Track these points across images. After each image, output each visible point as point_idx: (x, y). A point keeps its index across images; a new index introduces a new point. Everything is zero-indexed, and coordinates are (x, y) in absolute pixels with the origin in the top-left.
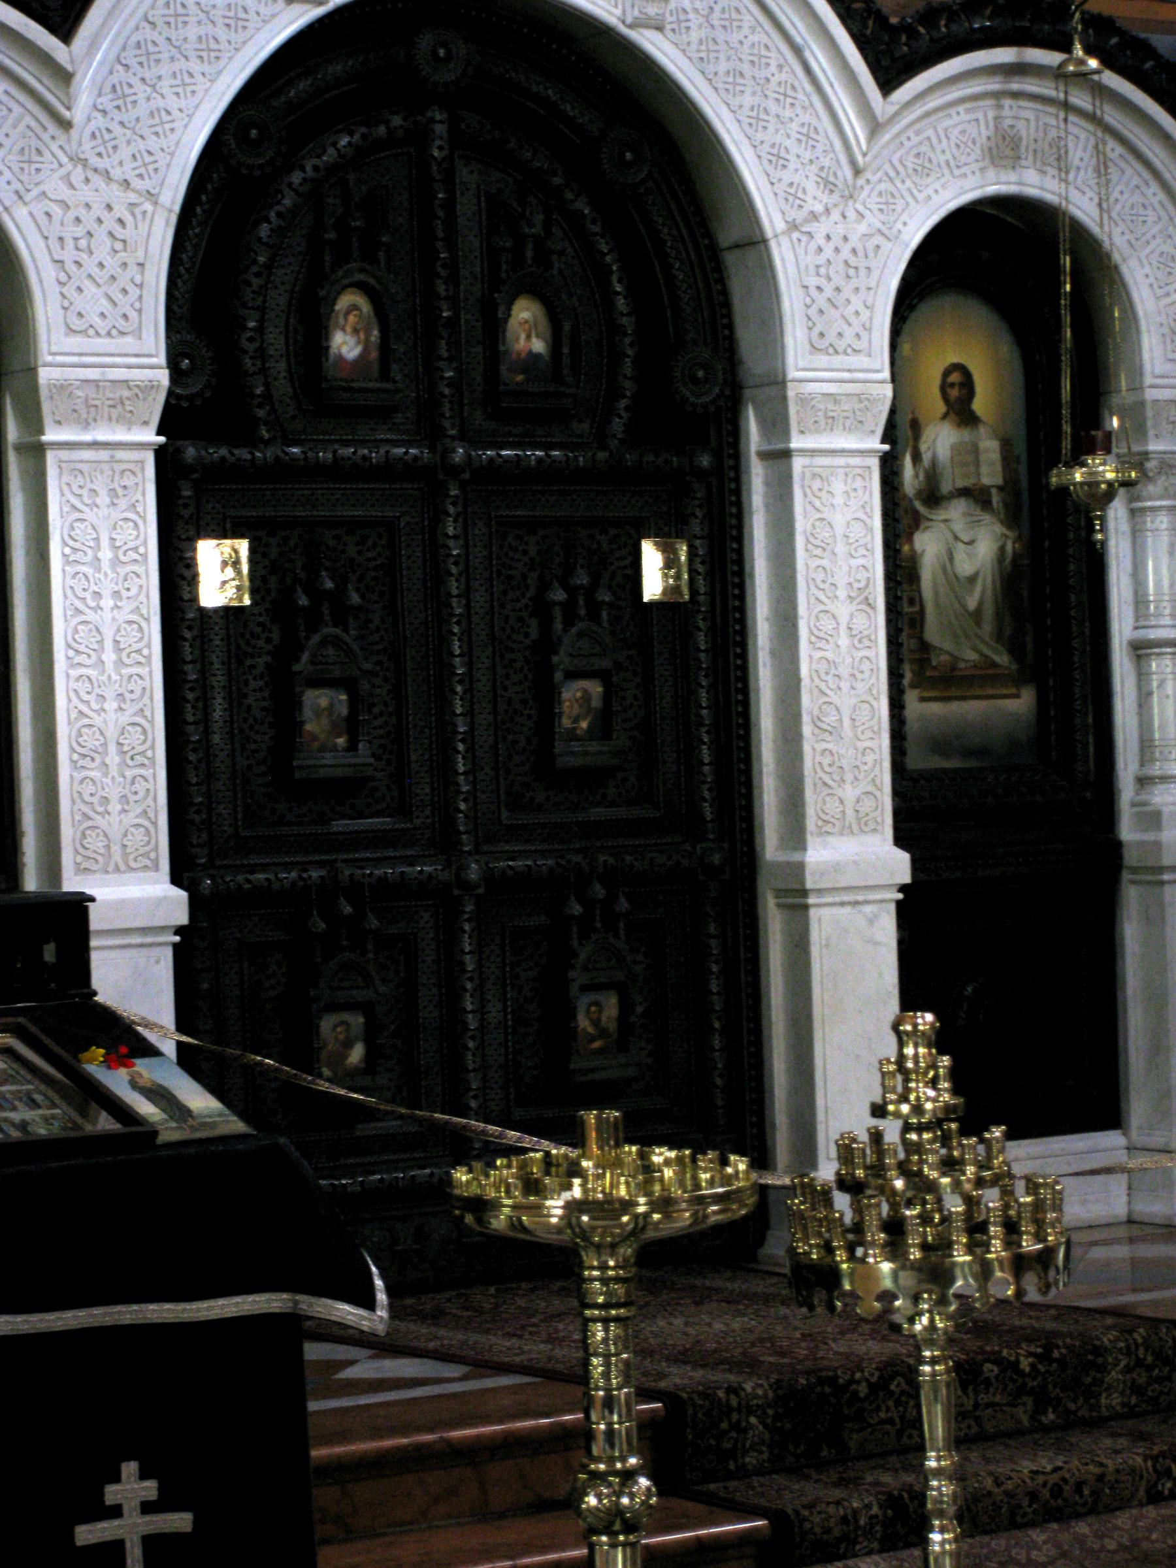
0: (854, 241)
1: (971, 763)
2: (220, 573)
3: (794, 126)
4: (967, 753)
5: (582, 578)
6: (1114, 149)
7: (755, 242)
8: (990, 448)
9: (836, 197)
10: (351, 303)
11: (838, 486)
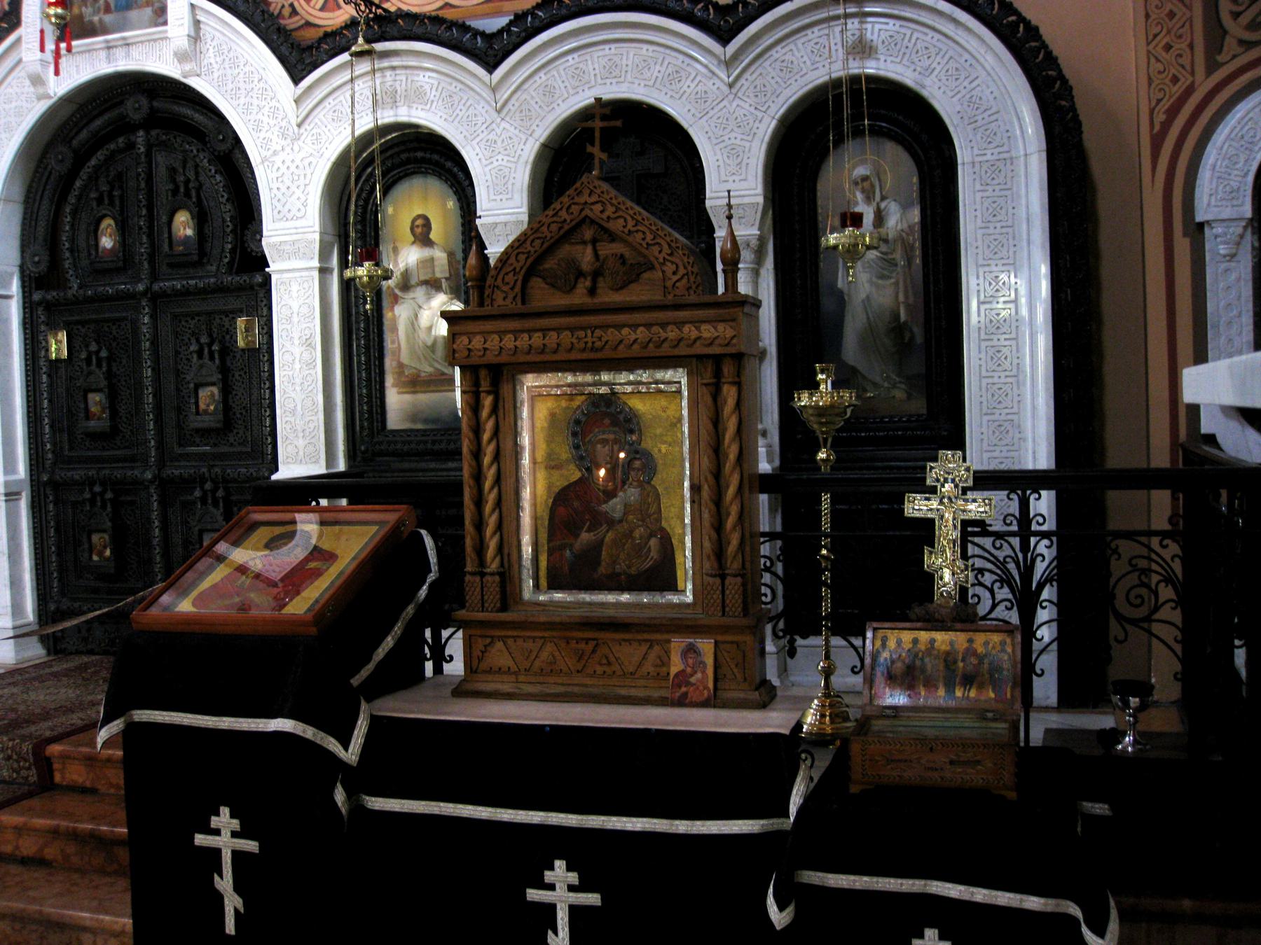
0: (298, 162)
1: (434, 427)
2: (58, 346)
3: (267, 109)
4: (426, 421)
5: (93, 347)
8: (440, 255)
9: (289, 141)
10: (108, 223)
11: (295, 287)
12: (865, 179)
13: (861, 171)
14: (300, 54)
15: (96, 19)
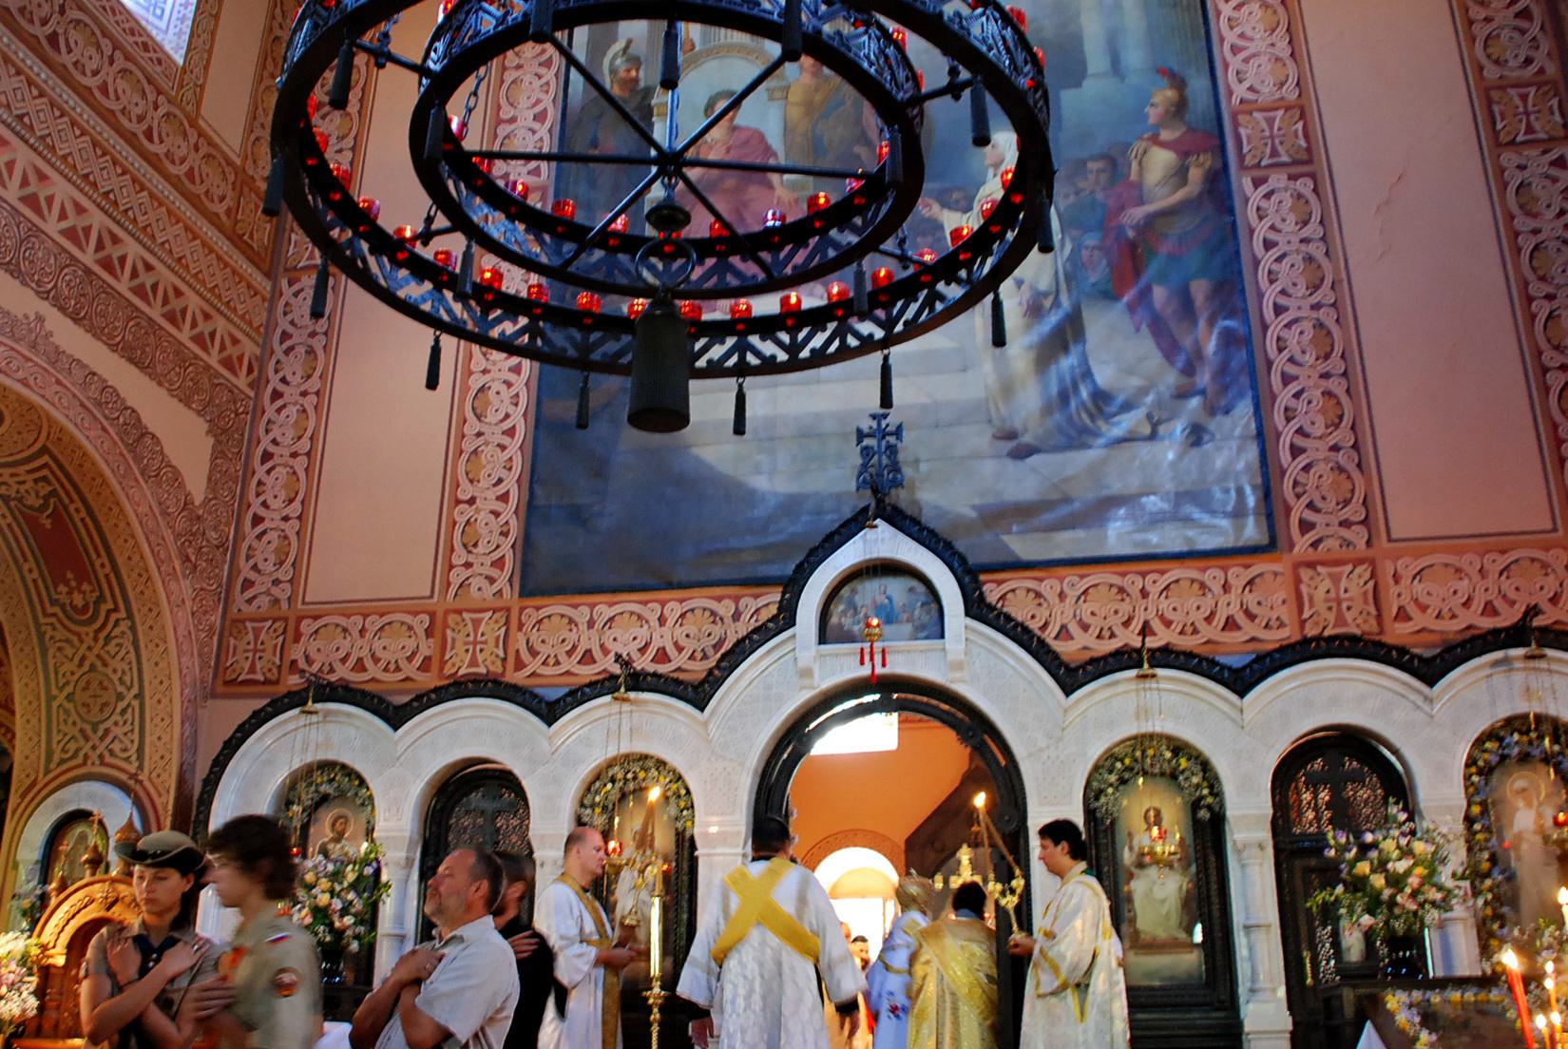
4: (1162, 979)
12: (1524, 790)
13: (1520, 784)
14: (1070, 677)
15: (856, 628)
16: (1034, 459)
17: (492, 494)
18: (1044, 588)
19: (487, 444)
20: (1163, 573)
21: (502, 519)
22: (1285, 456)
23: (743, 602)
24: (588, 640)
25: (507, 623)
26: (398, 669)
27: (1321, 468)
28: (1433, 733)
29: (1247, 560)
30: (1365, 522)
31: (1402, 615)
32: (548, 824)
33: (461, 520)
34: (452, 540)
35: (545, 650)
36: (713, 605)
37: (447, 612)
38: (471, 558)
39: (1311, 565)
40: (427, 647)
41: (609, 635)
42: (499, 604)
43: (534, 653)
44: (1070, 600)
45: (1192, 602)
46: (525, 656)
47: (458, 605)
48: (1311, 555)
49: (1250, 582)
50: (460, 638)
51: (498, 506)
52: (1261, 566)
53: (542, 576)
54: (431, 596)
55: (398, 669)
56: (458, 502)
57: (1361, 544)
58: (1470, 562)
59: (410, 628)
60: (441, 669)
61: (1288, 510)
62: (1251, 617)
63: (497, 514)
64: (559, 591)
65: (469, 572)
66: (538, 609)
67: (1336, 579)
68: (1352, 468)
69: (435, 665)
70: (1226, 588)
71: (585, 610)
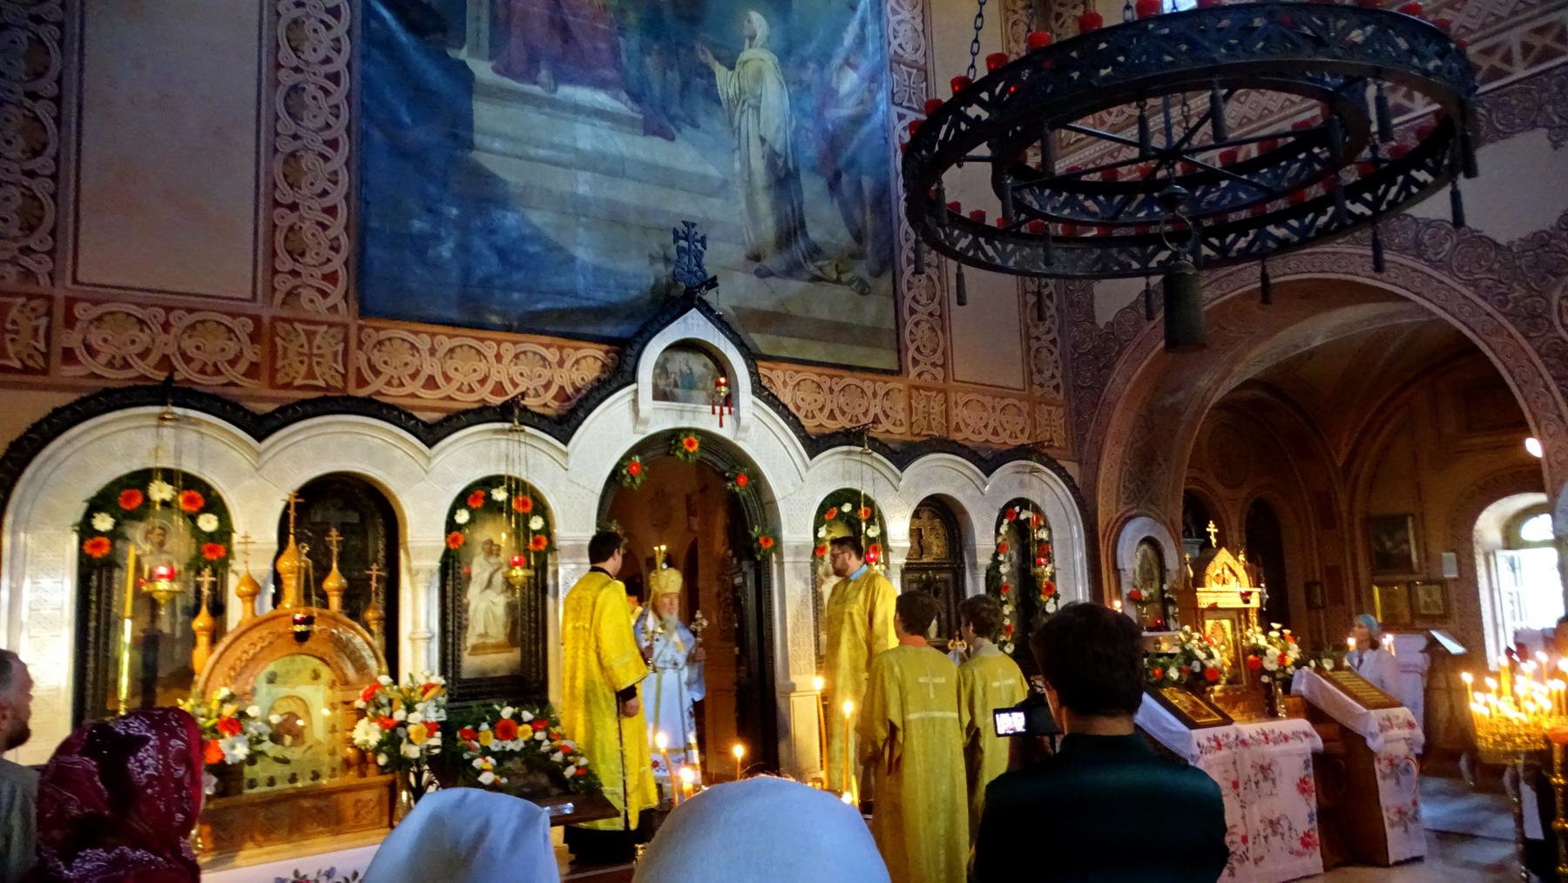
6: (877, 475)
7: (773, 502)
14: (815, 444)
16: (772, 281)
17: (317, 204)
18: (773, 375)
19: (306, 149)
20: (841, 377)
21: (331, 233)
22: (906, 311)
23: (567, 351)
24: (431, 367)
25: (346, 340)
26: (218, 372)
27: (924, 326)
28: (981, 501)
29: (885, 378)
30: (943, 366)
31: (958, 429)
32: (423, 536)
33: (283, 225)
34: (278, 247)
35: (388, 371)
36: (543, 351)
37: (274, 319)
38: (298, 267)
39: (917, 388)
40: (251, 354)
41: (450, 365)
42: (336, 318)
43: (377, 373)
44: (790, 388)
45: (857, 401)
46: (367, 374)
47: (286, 313)
48: (918, 382)
49: (887, 394)
50: (293, 348)
51: (326, 219)
52: (896, 384)
53: (380, 296)
54: (254, 298)
55: (218, 372)
56: (277, 204)
57: (941, 378)
58: (987, 400)
59: (230, 330)
60: (272, 376)
61: (907, 349)
62: (887, 416)
63: (324, 227)
64: (396, 316)
65: (298, 281)
66: (377, 330)
67: (929, 398)
68: (938, 329)
69: (265, 371)
70: (875, 395)
71: (426, 338)
